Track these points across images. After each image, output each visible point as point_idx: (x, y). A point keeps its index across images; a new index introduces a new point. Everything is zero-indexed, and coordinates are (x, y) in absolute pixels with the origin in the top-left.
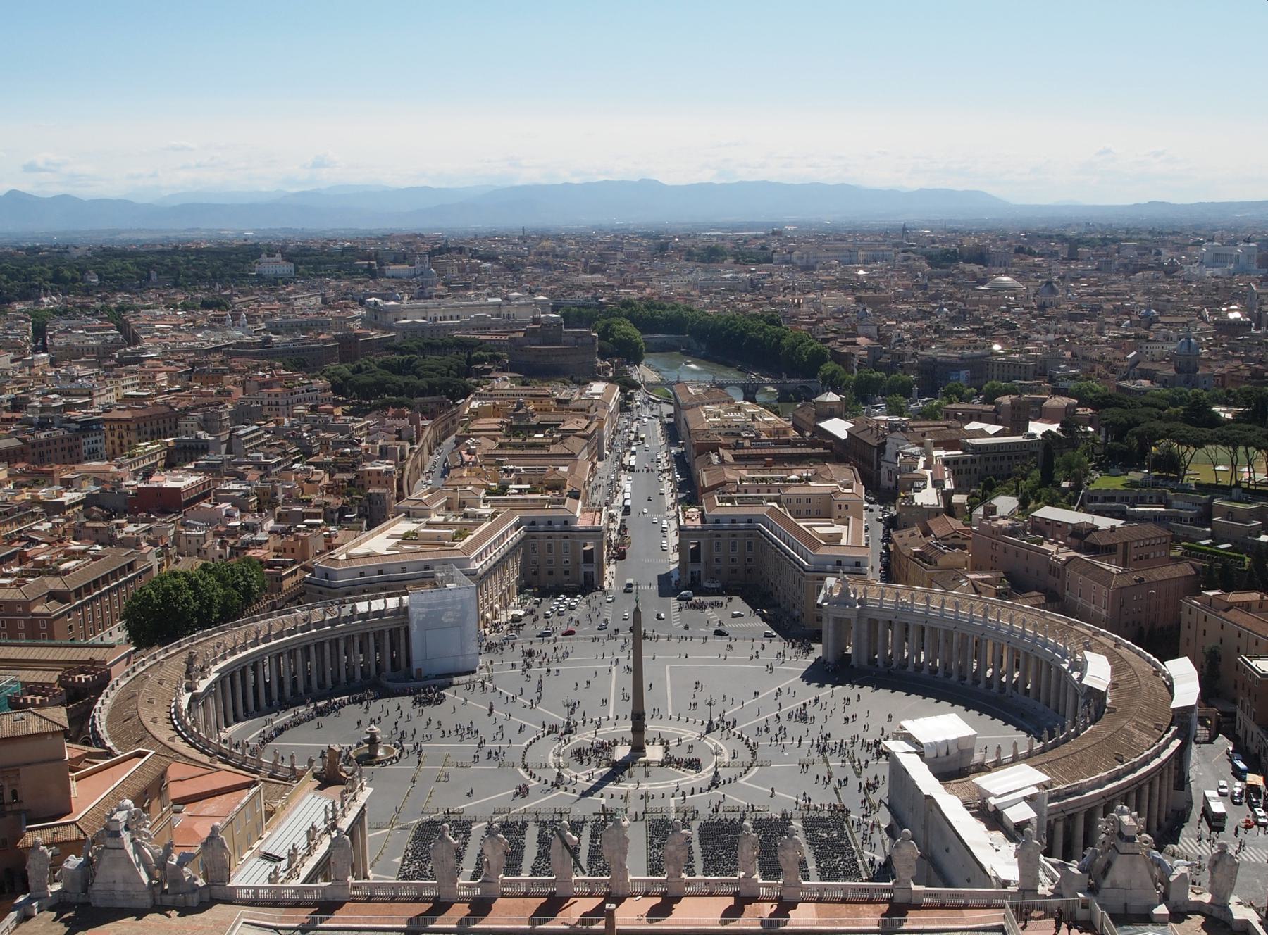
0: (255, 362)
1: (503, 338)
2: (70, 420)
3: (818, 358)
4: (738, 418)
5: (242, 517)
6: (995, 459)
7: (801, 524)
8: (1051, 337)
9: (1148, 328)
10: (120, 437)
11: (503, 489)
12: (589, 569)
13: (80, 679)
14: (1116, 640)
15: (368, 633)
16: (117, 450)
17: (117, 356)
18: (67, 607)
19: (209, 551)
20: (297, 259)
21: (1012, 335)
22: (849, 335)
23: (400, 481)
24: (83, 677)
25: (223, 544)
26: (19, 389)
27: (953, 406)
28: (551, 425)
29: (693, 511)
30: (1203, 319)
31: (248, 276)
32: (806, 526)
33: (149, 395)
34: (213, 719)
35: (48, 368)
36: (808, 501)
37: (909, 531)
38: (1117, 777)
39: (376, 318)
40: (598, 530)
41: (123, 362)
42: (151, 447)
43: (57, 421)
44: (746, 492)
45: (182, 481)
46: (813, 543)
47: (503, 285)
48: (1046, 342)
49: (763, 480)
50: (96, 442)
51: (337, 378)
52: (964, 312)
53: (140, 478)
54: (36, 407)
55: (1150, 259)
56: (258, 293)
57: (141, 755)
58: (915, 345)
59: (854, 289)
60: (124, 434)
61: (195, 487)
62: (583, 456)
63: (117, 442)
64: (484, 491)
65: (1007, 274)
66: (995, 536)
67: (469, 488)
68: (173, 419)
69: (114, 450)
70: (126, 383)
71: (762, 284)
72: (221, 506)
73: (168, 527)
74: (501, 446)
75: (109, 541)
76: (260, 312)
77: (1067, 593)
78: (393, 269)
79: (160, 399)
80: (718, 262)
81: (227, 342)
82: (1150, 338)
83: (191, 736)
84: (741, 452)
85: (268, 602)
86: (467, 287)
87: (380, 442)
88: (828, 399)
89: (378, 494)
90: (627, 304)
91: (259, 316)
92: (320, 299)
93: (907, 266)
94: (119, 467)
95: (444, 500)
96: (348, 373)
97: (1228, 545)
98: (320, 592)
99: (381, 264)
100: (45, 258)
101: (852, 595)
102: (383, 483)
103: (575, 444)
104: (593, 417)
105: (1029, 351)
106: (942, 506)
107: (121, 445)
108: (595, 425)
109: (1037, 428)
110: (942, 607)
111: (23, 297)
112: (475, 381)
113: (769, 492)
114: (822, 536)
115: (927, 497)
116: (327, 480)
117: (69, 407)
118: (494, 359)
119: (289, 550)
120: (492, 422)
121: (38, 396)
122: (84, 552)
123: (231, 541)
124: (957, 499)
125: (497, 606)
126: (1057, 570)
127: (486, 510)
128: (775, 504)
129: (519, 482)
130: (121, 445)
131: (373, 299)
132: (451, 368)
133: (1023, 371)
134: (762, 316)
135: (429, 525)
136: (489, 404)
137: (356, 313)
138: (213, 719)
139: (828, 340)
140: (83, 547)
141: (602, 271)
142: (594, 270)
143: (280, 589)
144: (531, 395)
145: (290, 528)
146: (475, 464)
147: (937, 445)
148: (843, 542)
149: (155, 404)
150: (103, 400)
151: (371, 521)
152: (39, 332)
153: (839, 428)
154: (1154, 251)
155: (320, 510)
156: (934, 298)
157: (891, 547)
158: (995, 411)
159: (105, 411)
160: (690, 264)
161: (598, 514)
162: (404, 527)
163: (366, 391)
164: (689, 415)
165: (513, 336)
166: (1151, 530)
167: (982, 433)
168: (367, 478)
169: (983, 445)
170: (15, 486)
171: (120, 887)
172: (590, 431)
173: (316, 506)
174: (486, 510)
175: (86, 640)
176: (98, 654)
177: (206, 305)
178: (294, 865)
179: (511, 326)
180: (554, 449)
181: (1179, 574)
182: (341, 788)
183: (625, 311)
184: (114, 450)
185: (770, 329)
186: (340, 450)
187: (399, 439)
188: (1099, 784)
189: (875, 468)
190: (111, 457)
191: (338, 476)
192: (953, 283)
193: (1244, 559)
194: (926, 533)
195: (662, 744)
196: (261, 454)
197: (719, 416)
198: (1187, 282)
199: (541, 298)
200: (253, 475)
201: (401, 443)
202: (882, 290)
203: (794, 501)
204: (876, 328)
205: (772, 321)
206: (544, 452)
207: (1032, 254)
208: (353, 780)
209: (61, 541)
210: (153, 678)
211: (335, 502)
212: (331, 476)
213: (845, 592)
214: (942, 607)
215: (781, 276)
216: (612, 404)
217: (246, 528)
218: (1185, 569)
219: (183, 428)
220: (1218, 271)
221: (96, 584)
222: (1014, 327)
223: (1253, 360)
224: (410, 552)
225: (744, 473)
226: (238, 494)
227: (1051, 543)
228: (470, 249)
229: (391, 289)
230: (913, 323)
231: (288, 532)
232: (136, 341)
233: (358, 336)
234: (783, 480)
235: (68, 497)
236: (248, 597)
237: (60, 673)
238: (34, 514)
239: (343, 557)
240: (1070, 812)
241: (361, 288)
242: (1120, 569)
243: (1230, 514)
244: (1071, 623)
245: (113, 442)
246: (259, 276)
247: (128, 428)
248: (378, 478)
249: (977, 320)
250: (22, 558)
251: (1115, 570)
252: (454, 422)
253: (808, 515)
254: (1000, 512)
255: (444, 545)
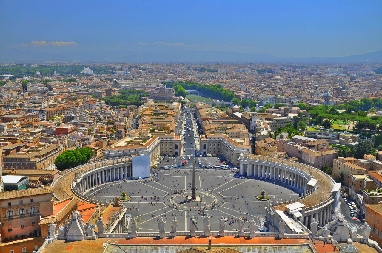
0: (85, 96)
1: (149, 90)
2: (36, 110)
3: (232, 97)
4: (213, 112)
5: (85, 136)
6: (280, 123)
7: (233, 139)
8: (291, 92)
9: (316, 90)
10: (50, 115)
11: (153, 130)
12: (177, 151)
13: (45, 179)
14: (317, 170)
15: (121, 167)
16: (49, 118)
17: (47, 93)
18: (40, 160)
19: (76, 145)
20: (94, 69)
21: (281, 91)
22: (239, 91)
23: (125, 127)
24: (46, 178)
25: (80, 143)
26: (21, 102)
27: (268, 109)
28: (164, 113)
29: (204, 136)
30: (330, 87)
31: (80, 73)
32: (234, 140)
33: (57, 104)
34: (81, 189)
35: (28, 96)
36: (234, 133)
37: (260, 141)
38: (321, 205)
39: (116, 84)
40: (179, 140)
41: (49, 95)
42: (58, 118)
43: (32, 110)
44: (217, 131)
45: (68, 126)
46: (236, 144)
47: (148, 76)
48: (290, 93)
49: (221, 128)
50: (43, 116)
51: (107, 100)
52: (268, 85)
53: (56, 126)
54: (26, 107)
55: (314, 72)
56: (83, 78)
57: (71, 199)
58: (256, 93)
59: (239, 79)
60: (51, 114)
61: (72, 128)
62: (173, 121)
63: (49, 116)
64: (149, 130)
65: (278, 75)
66: (283, 143)
67: (145, 129)
68: (64, 110)
69: (48, 118)
70: (50, 101)
71: (215, 77)
72: (79, 133)
73: (65, 139)
74: (152, 119)
75: (50, 143)
76: (84, 83)
77: (303, 158)
78: (118, 72)
79: (60, 105)
80: (203, 71)
81: (76, 90)
82: (317, 92)
83: (77, 194)
84: (214, 121)
85: (93, 159)
86: (138, 77)
87: (120, 117)
88: (236, 107)
89: (120, 131)
90: (180, 82)
91: (84, 84)
92: (100, 79)
93: (252, 73)
94: (50, 123)
95: (139, 132)
96: (109, 99)
97: (344, 146)
98: (108, 156)
99: (115, 71)
100: (25, 67)
101: (248, 158)
102: (121, 128)
103: (171, 118)
104: (175, 111)
105: (286, 95)
106: (268, 135)
107: (50, 117)
108: (176, 113)
109: (291, 115)
110: (271, 161)
111: (20, 77)
112: (142, 101)
113: (223, 131)
114: (238, 143)
115: (264, 133)
116: (106, 127)
117: (35, 107)
118: (147, 96)
119: (98, 145)
120: (149, 112)
121: (27, 104)
122: (44, 145)
123: (82, 143)
124: (272, 133)
125: (154, 160)
126: (300, 152)
127: (150, 135)
128: (225, 134)
129: (158, 128)
130: (50, 117)
131: (115, 80)
132: (136, 98)
133: (285, 101)
134: (216, 85)
135: (136, 139)
136: (148, 107)
137: (110, 83)
138: (81, 189)
139: (234, 92)
140: (44, 144)
141: (174, 74)
142: (171, 73)
143: (96, 156)
144: (159, 106)
145: (98, 139)
146: (146, 123)
147: (266, 119)
148: (244, 144)
149: (59, 106)
150: (44, 105)
151: (118, 138)
152: (25, 87)
153: (239, 115)
154: (315, 70)
155: (105, 135)
156: (260, 81)
157: (256, 145)
158: (279, 110)
159: (46, 108)
160: (196, 72)
161: (179, 137)
162: (129, 139)
163: (113, 104)
164: (200, 111)
165: (152, 90)
166: (324, 142)
167: (277, 116)
168: (117, 127)
169: (278, 119)
170: (22, 127)
171: (75, 234)
172: (175, 115)
173: (105, 134)
174: (150, 135)
175: (45, 168)
176: (50, 173)
177: (70, 80)
178: (109, 229)
179: (151, 87)
180: (166, 120)
181: (332, 153)
182: (121, 208)
183: (180, 84)
184: (48, 118)
185: (218, 89)
186: (109, 119)
187: (124, 116)
188: (317, 207)
189: (249, 125)
190: (47, 120)
191: (109, 126)
192: (265, 78)
193: (348, 149)
194: (265, 142)
195: (200, 196)
196: (88, 120)
197: (208, 111)
198: (325, 78)
199: (159, 80)
200: (86, 125)
201: (125, 117)
202: (246, 79)
203: (230, 133)
204: (246, 89)
205: (219, 87)
206: (163, 120)
207: (284, 70)
208: (122, 207)
209: (37, 142)
210: (65, 179)
211: (109, 133)
212: (107, 126)
213: (246, 157)
214: (271, 161)
215: (220, 75)
216: (180, 108)
217: (86, 139)
218: (333, 152)
219: (67, 113)
220: (332, 75)
221: (48, 153)
222: (281, 89)
223: (344, 98)
224: (131, 146)
225: (216, 126)
226: (83, 130)
227: (298, 145)
228: (139, 67)
229: (118, 77)
230: (255, 88)
231: (97, 140)
232: (51, 89)
233: (111, 89)
234: (226, 128)
235: (37, 131)
236: (89, 158)
237: (40, 177)
238: (28, 135)
239: (113, 147)
240: (310, 214)
241: (110, 77)
242: (317, 152)
243: (344, 137)
244: (305, 165)
245: (48, 116)
246: (83, 73)
247: (52, 113)
248: (120, 127)
249: (271, 87)
250: (26, 147)
251: (315, 152)
252: (138, 112)
253: (234, 137)
254: (284, 137)
255: (140, 144)
